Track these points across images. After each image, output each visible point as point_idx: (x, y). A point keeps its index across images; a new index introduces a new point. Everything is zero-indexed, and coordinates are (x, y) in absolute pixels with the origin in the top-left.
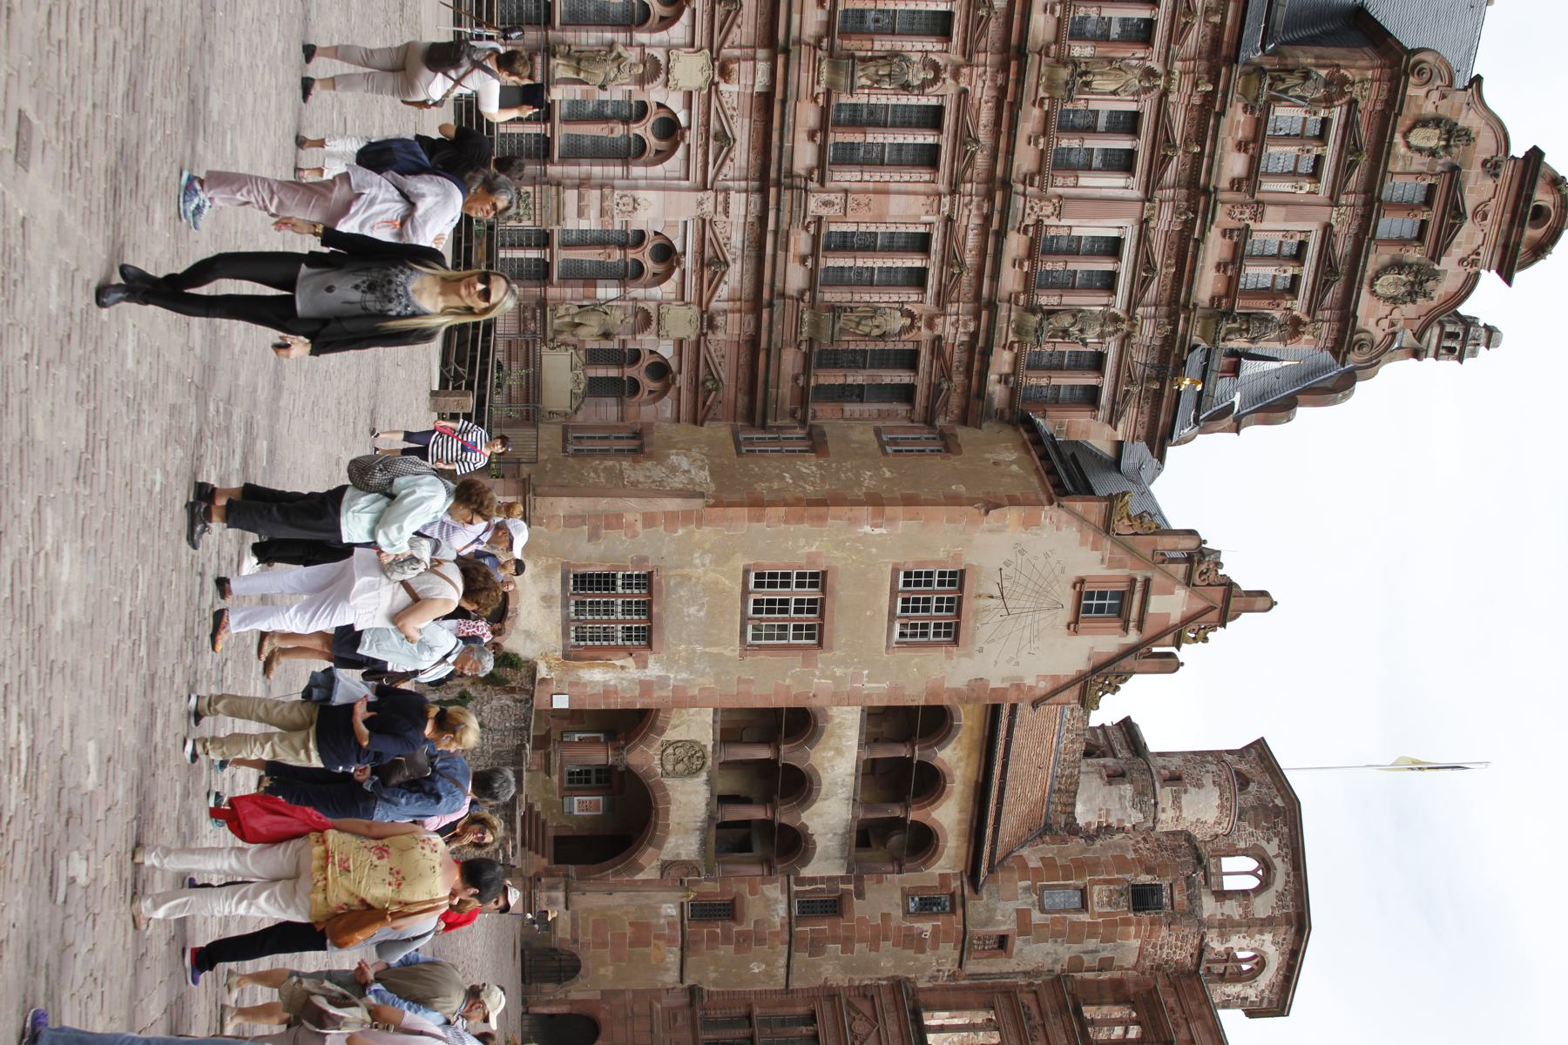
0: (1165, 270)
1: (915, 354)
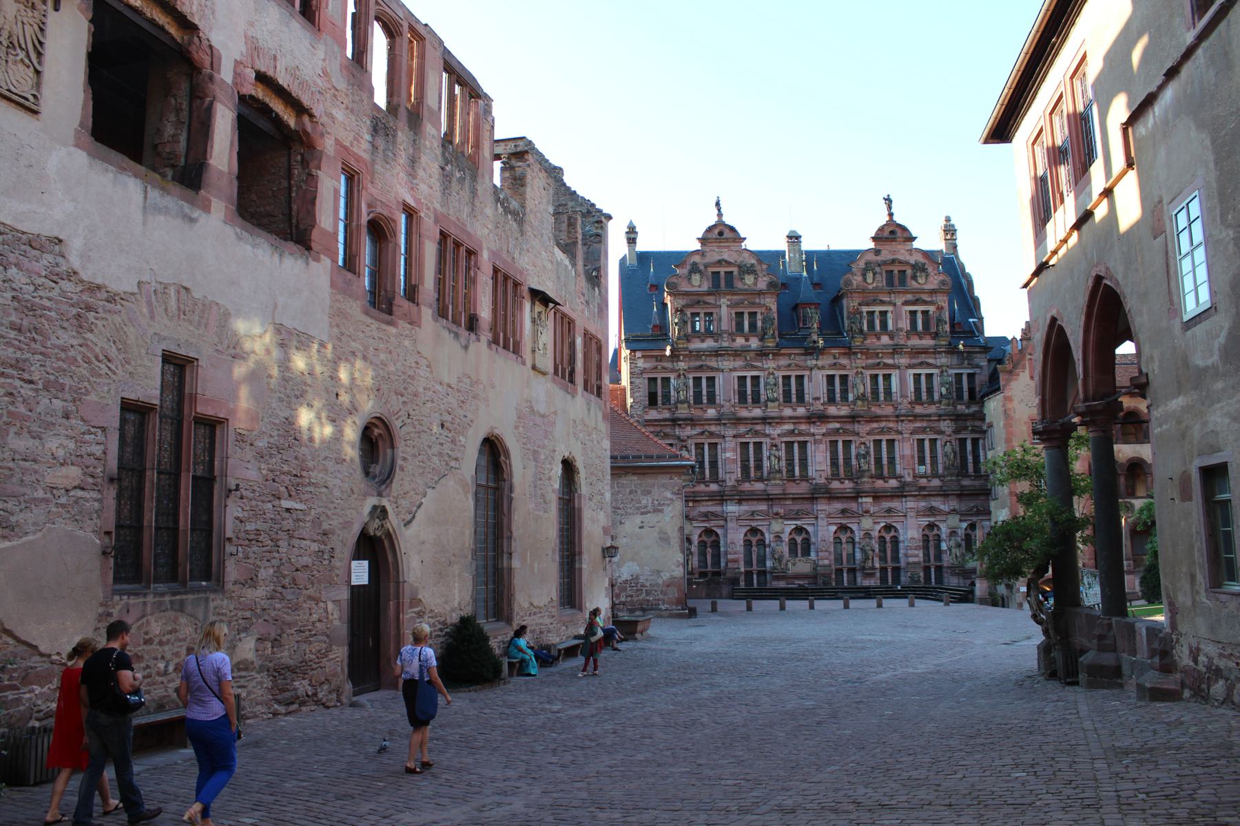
0: (923, 358)
1: (960, 439)
